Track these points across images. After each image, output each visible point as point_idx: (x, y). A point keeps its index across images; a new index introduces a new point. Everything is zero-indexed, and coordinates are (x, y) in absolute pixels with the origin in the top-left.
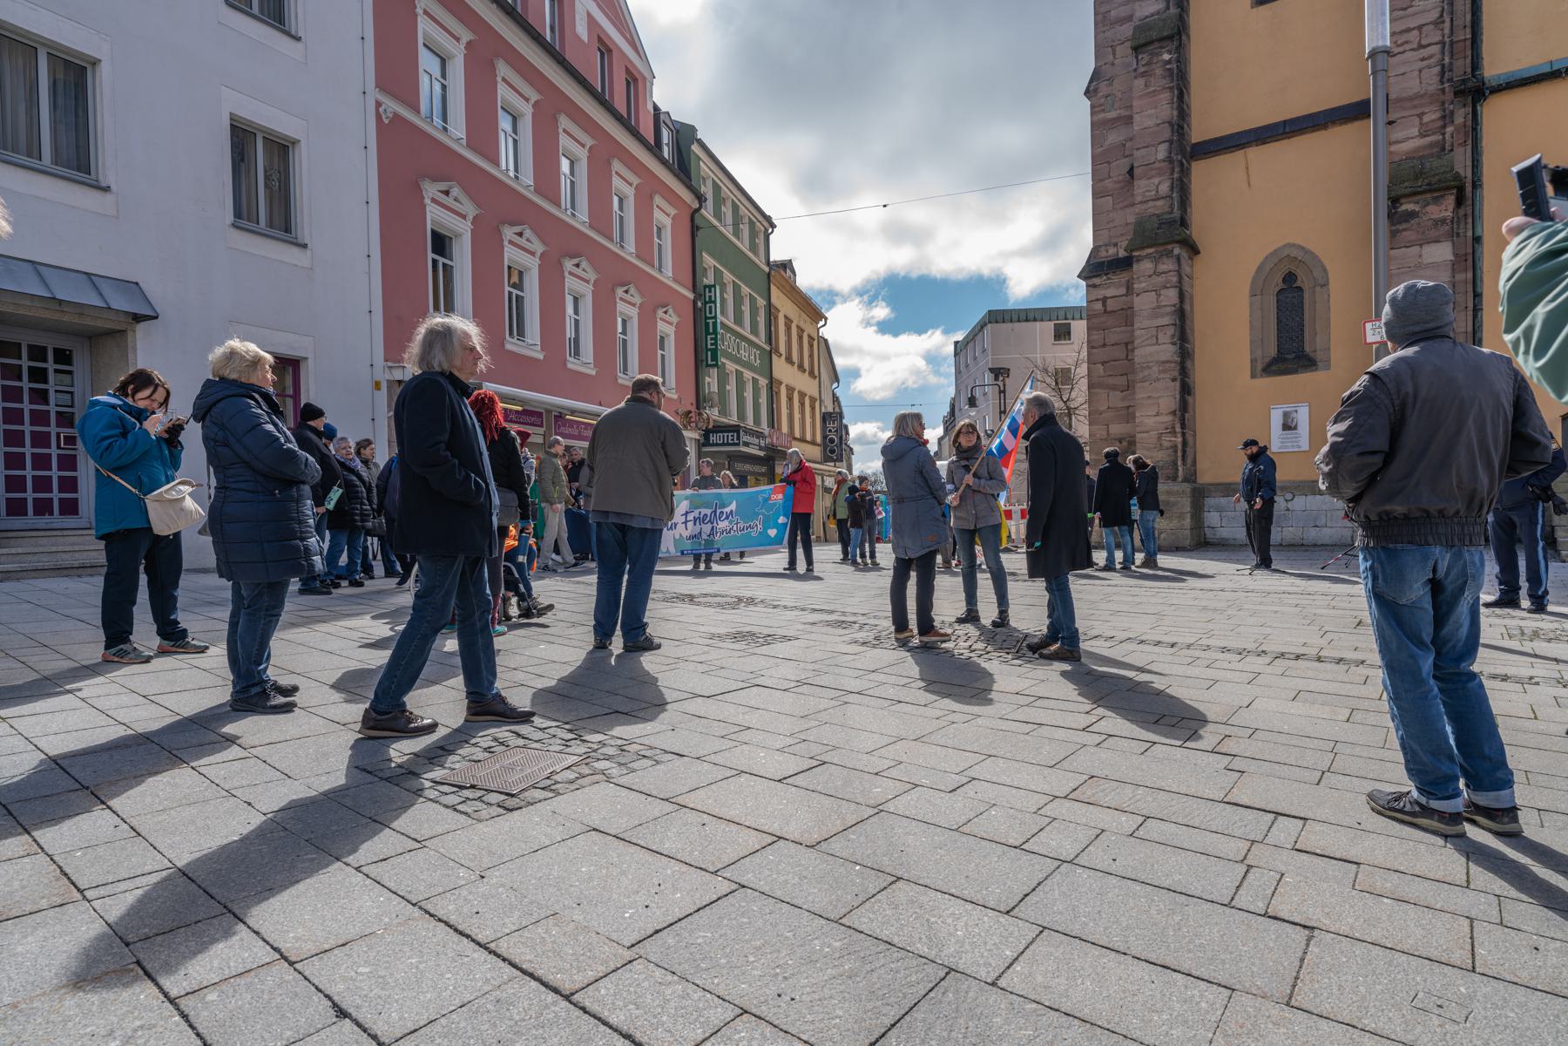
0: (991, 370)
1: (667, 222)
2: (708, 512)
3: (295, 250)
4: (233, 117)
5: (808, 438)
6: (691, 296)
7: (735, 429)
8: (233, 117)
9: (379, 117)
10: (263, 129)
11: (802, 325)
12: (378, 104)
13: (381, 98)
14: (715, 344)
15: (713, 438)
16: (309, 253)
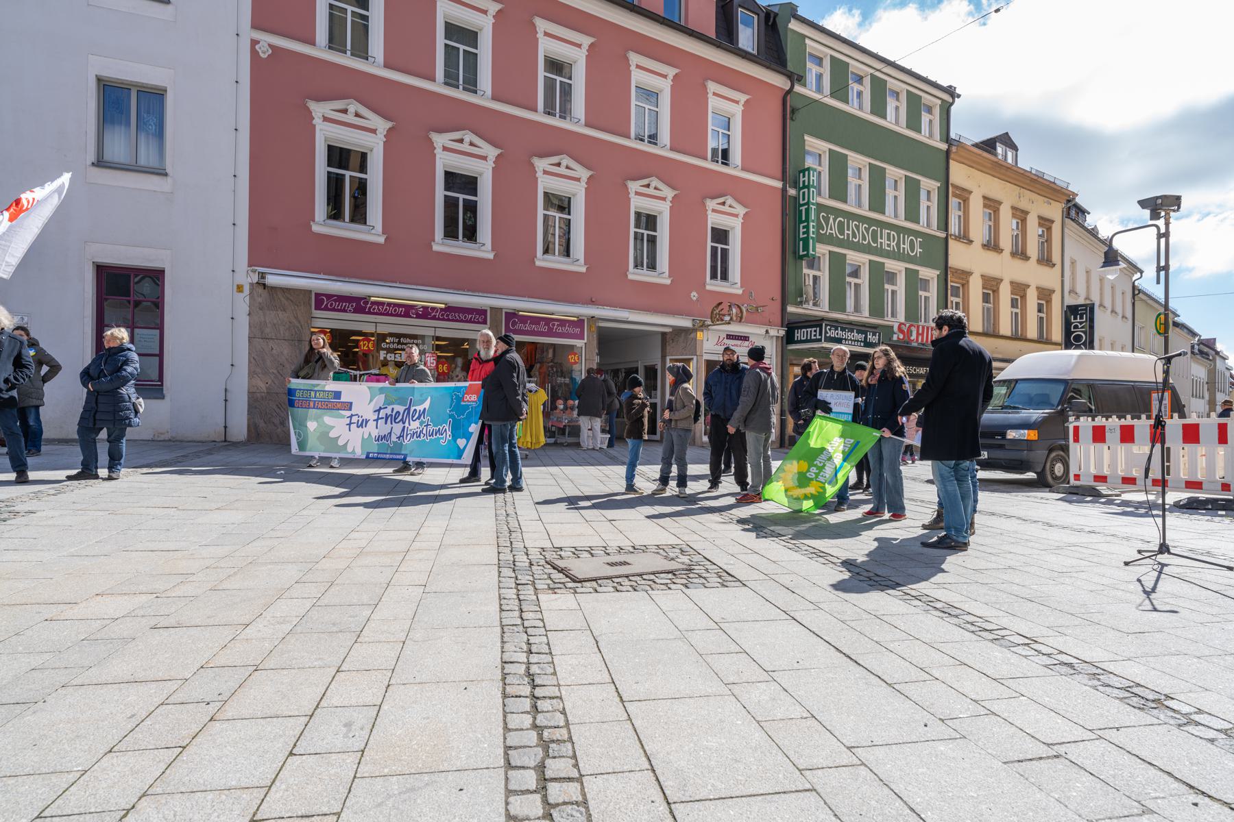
0: (1143, 204)
1: (737, 111)
2: (401, 409)
3: (155, 178)
4: (99, 80)
5: (1032, 332)
6: (779, 184)
7: (817, 323)
8: (99, 80)
9: (254, 53)
10: (135, 85)
11: (1023, 205)
12: (254, 43)
13: (258, 35)
14: (807, 232)
15: (799, 335)
16: (169, 179)
